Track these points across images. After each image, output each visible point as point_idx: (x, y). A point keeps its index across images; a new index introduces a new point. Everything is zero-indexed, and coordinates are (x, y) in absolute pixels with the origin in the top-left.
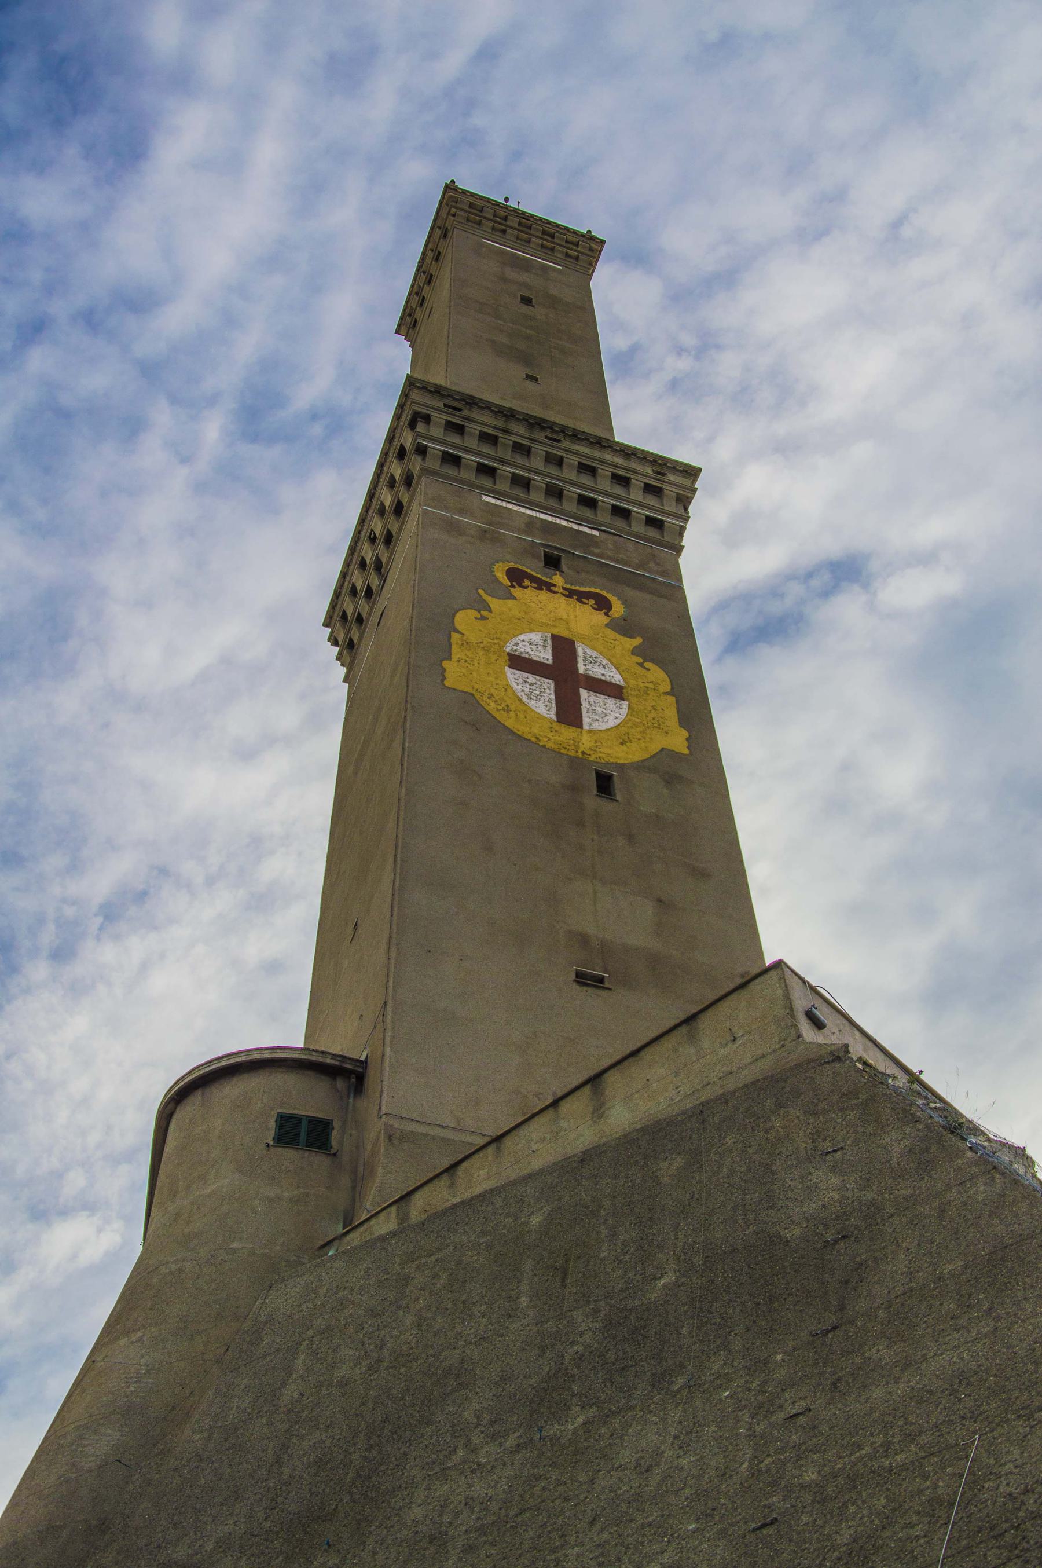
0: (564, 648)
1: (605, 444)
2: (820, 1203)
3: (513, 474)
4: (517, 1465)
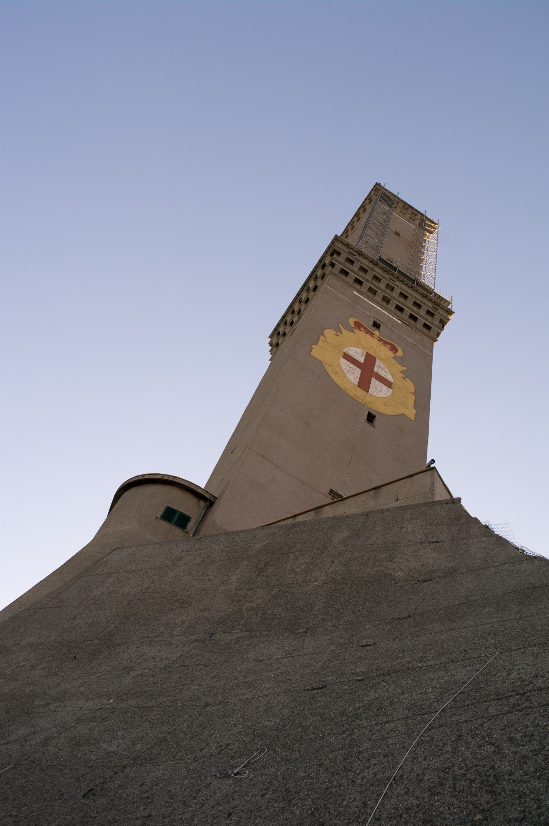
0: (370, 360)
1: (415, 283)
2: (420, 564)
3: (370, 287)
4: (191, 647)
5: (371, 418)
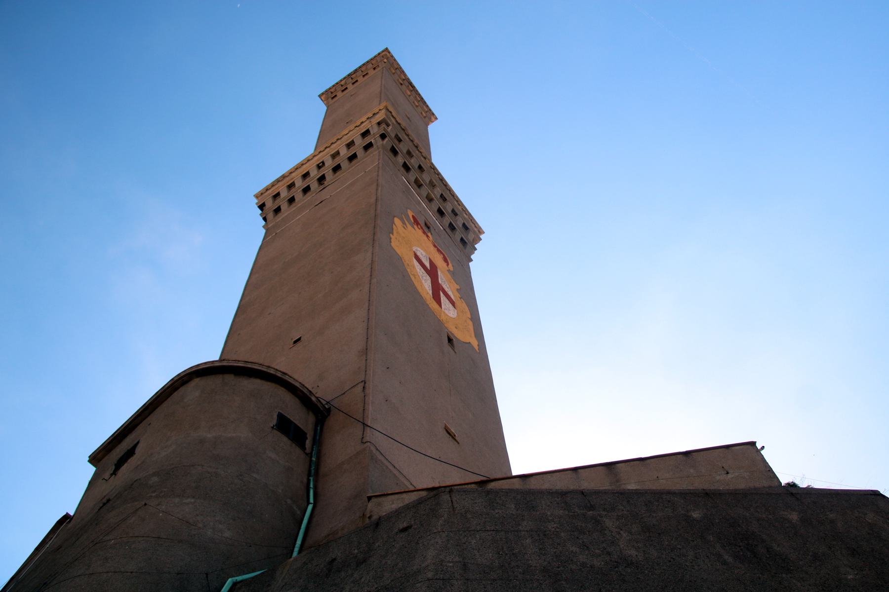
5: (450, 340)
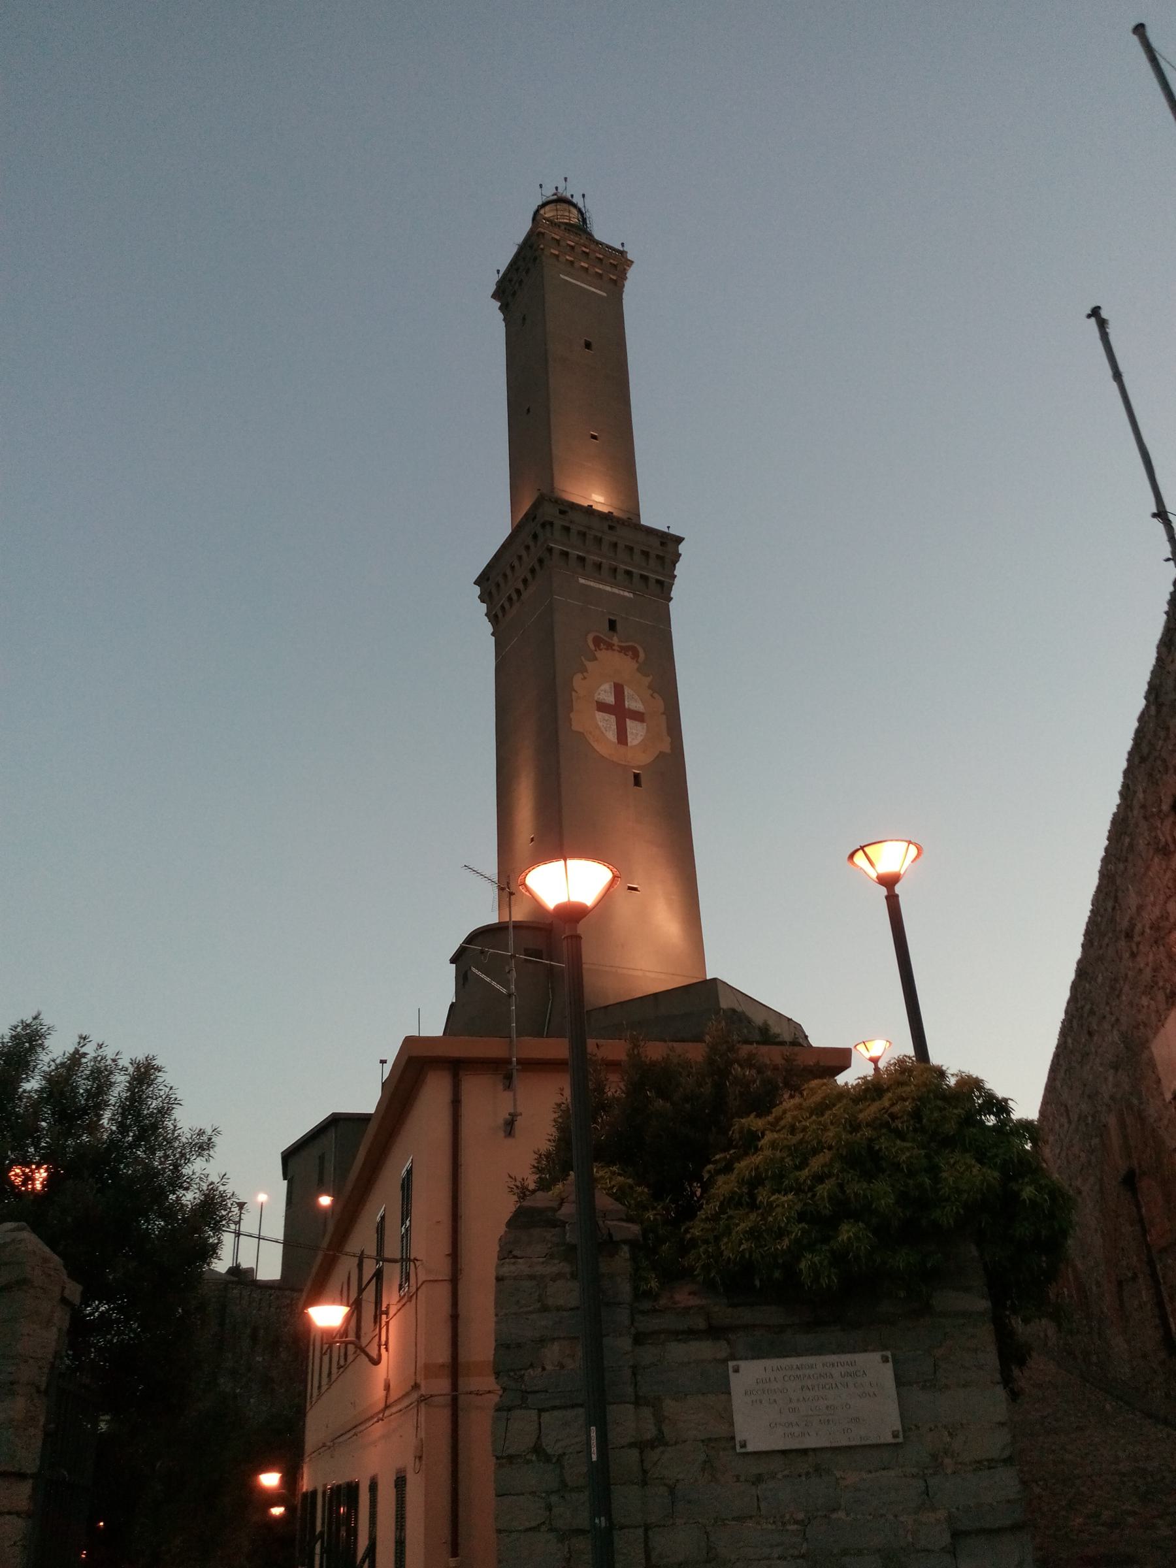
5: (637, 777)
